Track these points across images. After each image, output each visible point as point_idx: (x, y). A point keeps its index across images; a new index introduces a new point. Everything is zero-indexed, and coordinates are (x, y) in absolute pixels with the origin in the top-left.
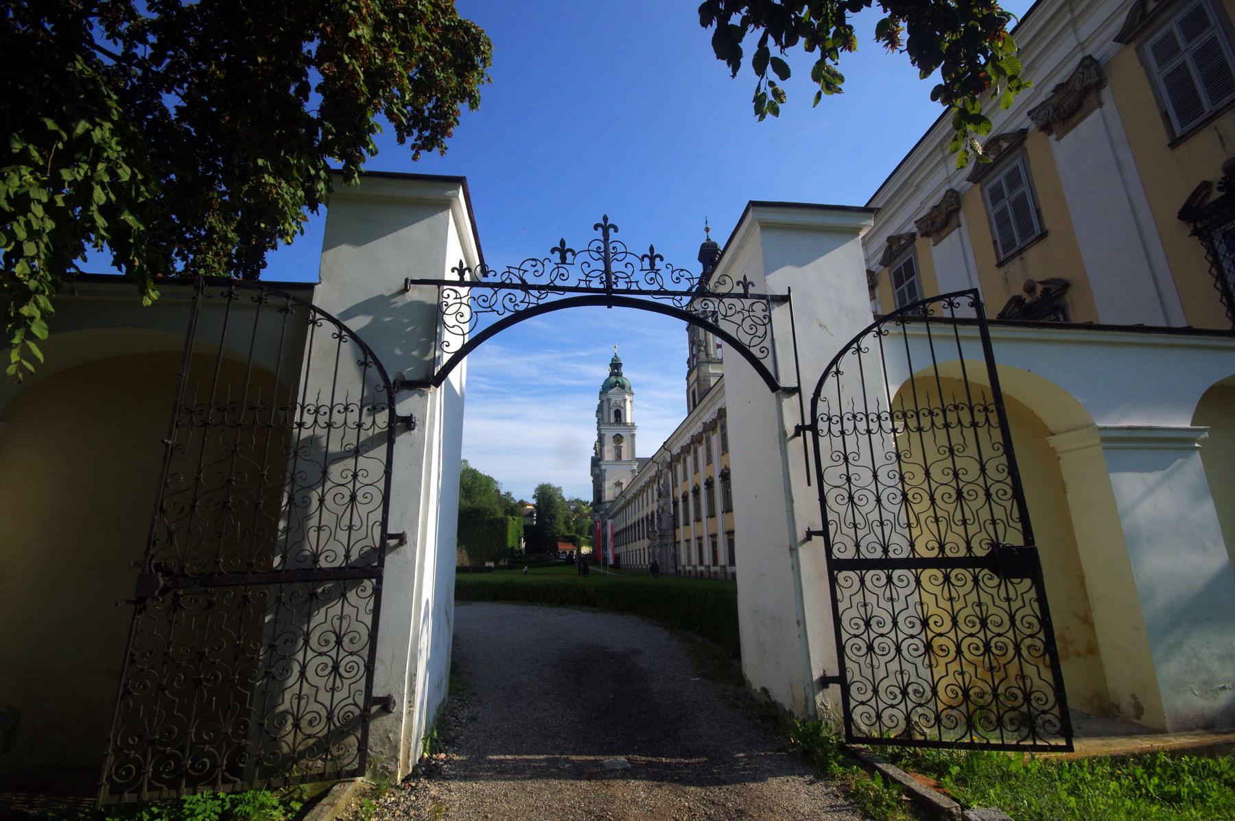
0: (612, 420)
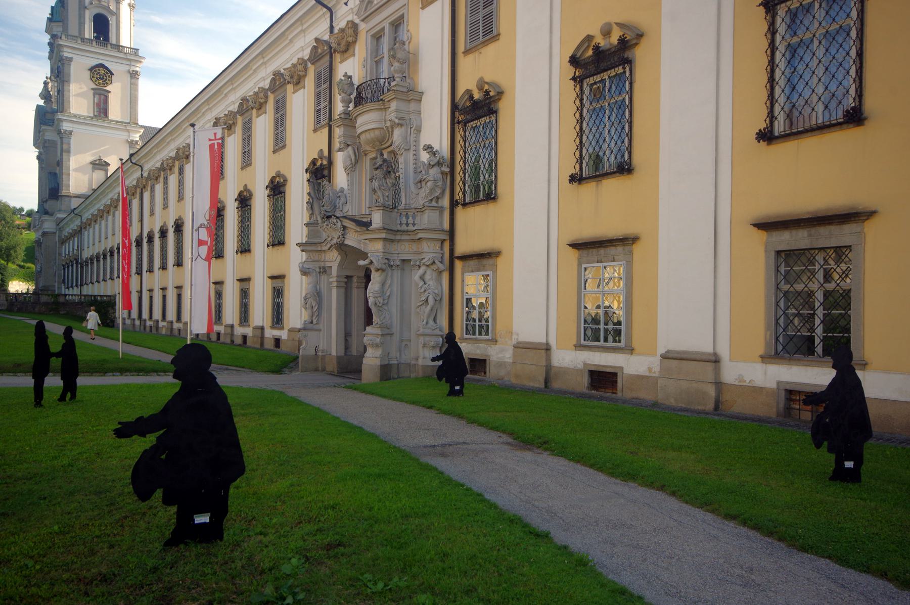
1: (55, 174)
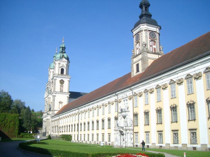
0: (60, 73)
1: (50, 105)
